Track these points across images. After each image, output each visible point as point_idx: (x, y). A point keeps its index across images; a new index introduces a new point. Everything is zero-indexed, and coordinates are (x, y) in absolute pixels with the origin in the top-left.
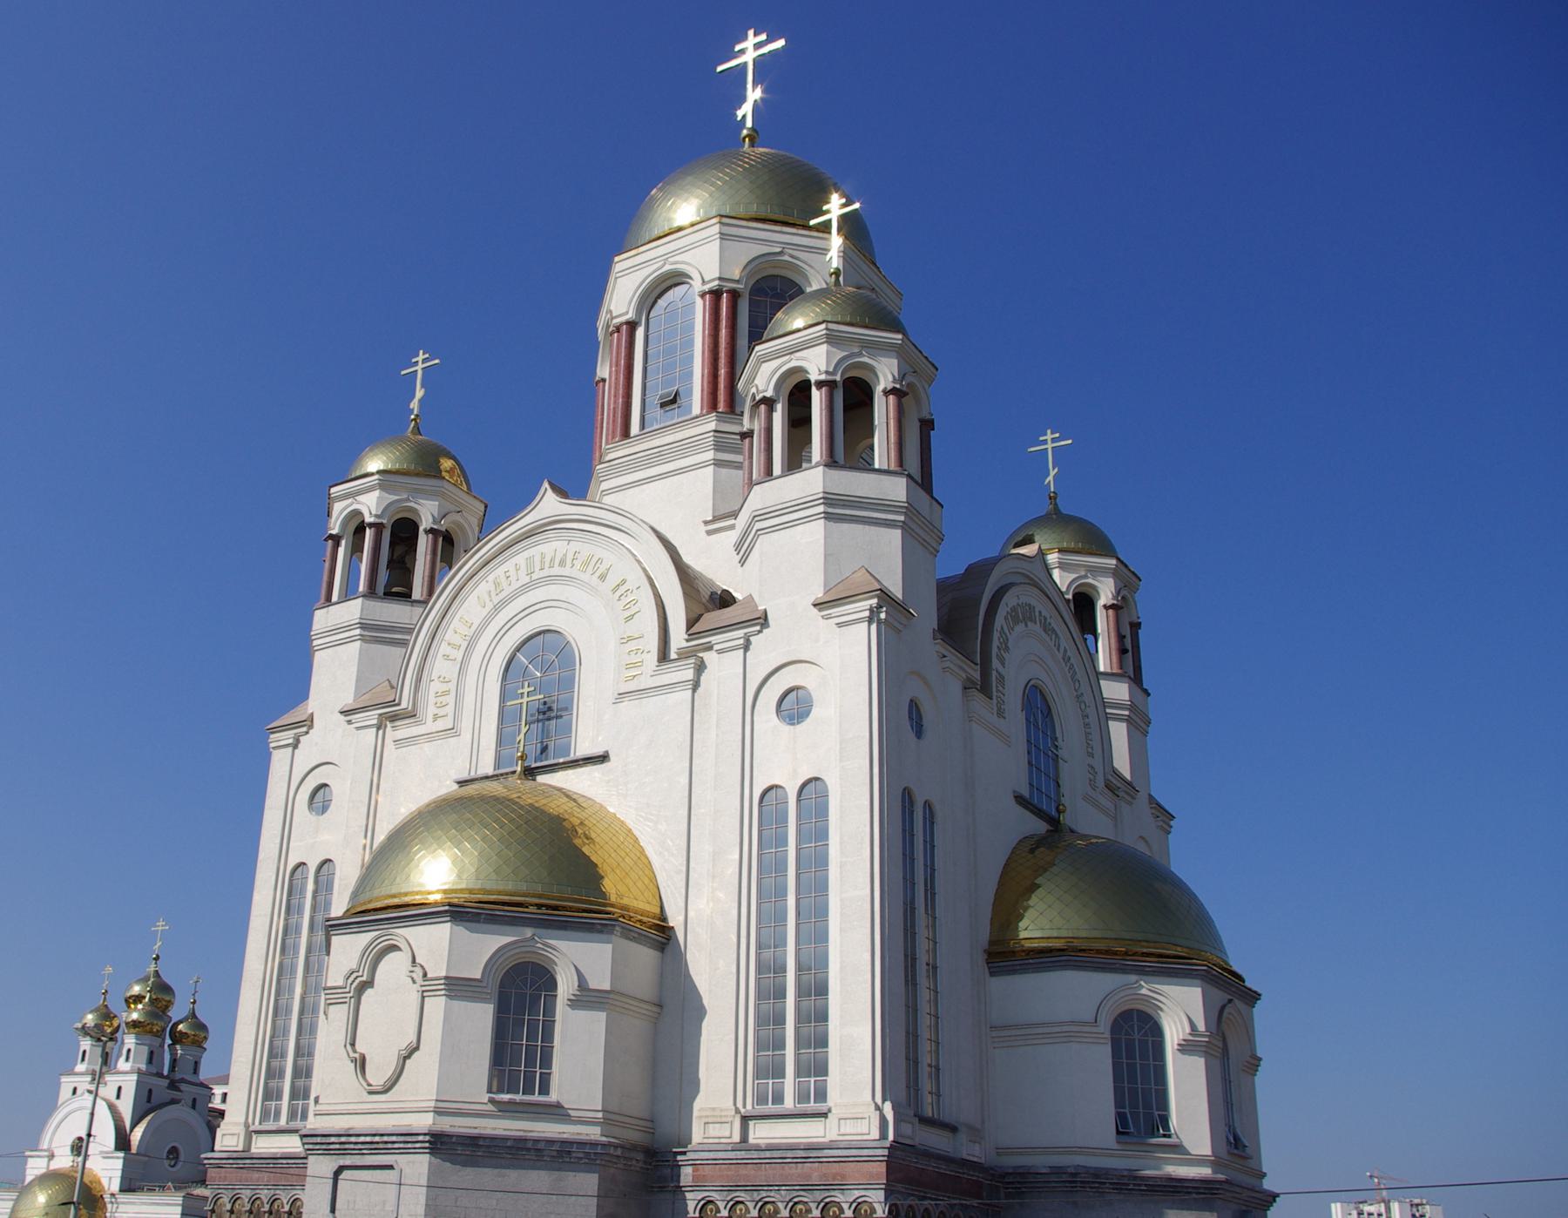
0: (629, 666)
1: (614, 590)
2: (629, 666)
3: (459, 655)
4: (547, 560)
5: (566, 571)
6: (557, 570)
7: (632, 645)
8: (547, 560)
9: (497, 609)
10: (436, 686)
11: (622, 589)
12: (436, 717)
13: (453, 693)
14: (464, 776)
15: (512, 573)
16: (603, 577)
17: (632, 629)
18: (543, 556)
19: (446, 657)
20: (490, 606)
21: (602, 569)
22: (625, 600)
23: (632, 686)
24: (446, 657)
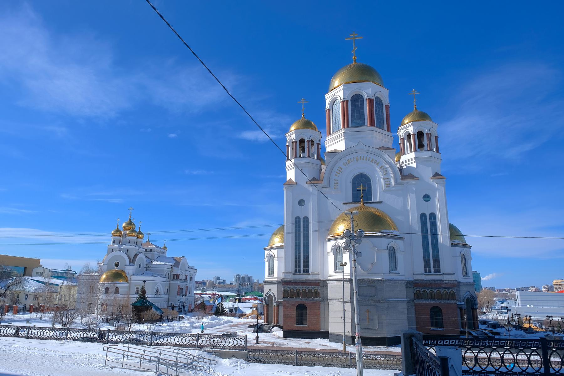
14: (344, 202)
15: (352, 159)
21: (377, 163)
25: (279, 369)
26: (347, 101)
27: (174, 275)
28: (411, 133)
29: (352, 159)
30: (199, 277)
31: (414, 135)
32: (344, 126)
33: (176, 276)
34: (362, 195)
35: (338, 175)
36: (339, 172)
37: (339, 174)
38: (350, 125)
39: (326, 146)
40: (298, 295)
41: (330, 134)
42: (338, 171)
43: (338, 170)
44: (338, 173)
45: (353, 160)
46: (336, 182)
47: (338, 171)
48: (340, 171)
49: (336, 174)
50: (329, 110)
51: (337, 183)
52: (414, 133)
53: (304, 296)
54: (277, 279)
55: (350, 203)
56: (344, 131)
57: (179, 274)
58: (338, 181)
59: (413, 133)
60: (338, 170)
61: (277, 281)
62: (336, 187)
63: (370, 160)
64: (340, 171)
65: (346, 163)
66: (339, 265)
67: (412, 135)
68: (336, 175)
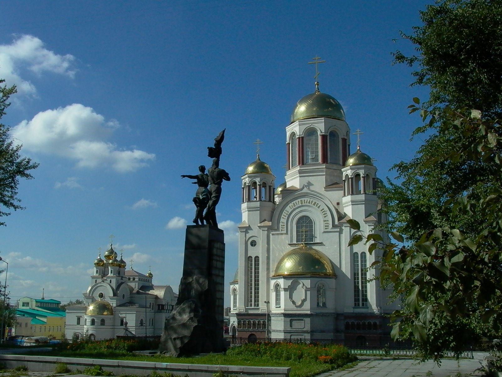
0: (326, 226)
1: (321, 210)
2: (326, 226)
3: (286, 218)
4: (306, 201)
5: (310, 205)
6: (308, 204)
7: (326, 222)
8: (306, 201)
9: (294, 210)
10: (281, 224)
11: (323, 211)
12: (282, 230)
13: (285, 226)
15: (297, 202)
16: (319, 207)
17: (326, 219)
18: (304, 200)
19: (283, 218)
20: (292, 209)
21: (318, 205)
22: (324, 213)
23: (326, 230)
24: (283, 218)
27: (159, 305)
29: (297, 202)
32: (299, 164)
33: (161, 306)
35: (285, 217)
37: (286, 216)
39: (287, 181)
41: (289, 169)
44: (285, 216)
45: (298, 204)
48: (287, 214)
50: (289, 144)
56: (299, 169)
57: (163, 304)
61: (236, 314)
62: (283, 229)
63: (313, 203)
65: (292, 206)
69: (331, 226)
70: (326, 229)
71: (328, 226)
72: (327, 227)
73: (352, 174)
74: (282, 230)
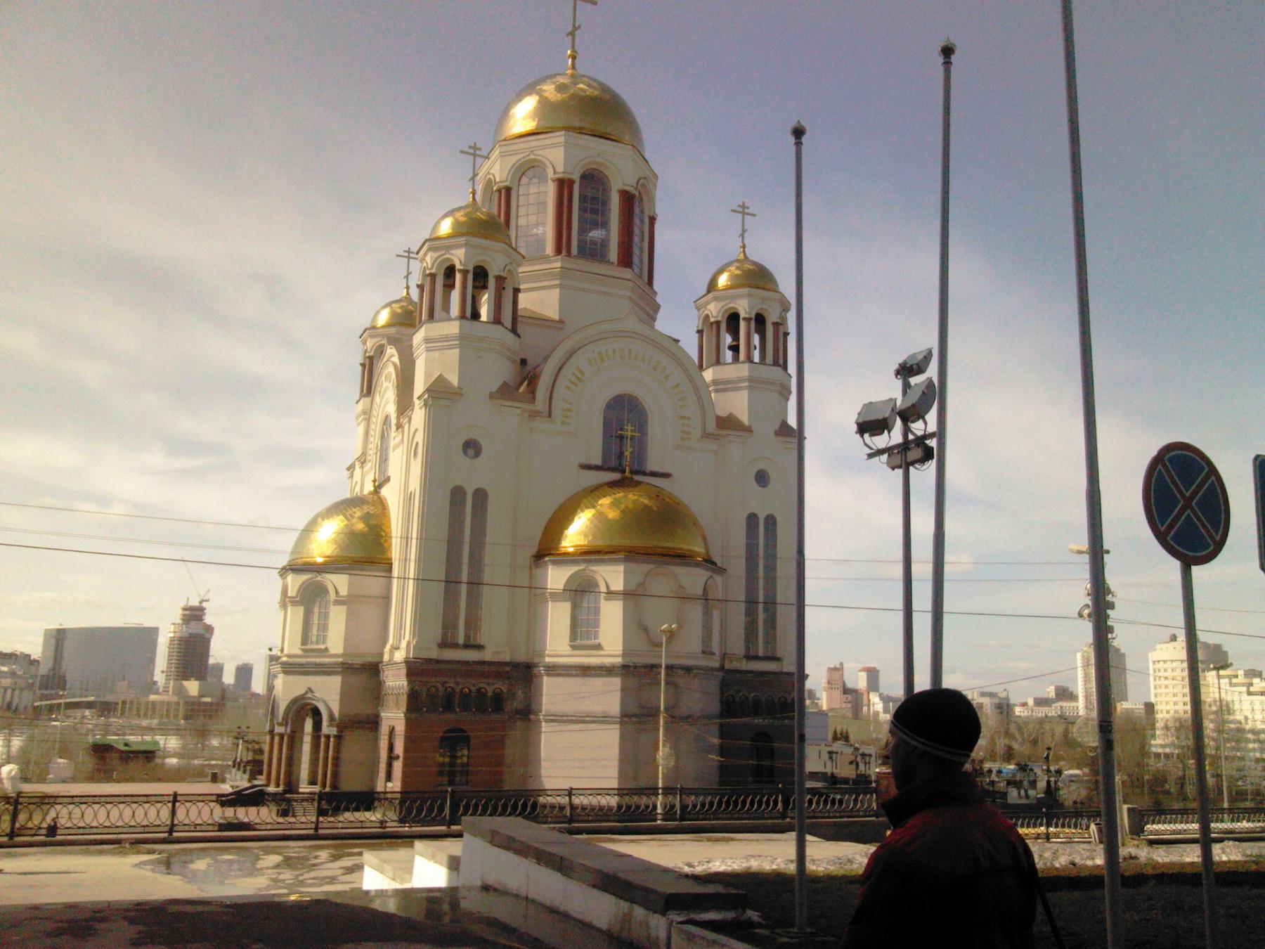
1: (673, 388)
2: (683, 432)
7: (685, 421)
14: (583, 461)
16: (667, 377)
18: (630, 351)
25: (848, 867)
26: (571, 182)
28: (458, 266)
30: (737, 645)
31: (748, 320)
32: (558, 251)
34: (630, 450)
36: (576, 381)
38: (574, 250)
40: (448, 705)
42: (574, 379)
43: (573, 374)
46: (567, 406)
47: (574, 379)
48: (579, 379)
49: (570, 385)
51: (569, 410)
52: (466, 268)
53: (465, 707)
54: (341, 660)
55: (597, 468)
58: (571, 404)
59: (462, 268)
60: (573, 374)
61: (342, 663)
64: (579, 379)
65: (595, 359)
66: (581, 629)
67: (460, 271)
68: (568, 388)
69: (696, 433)
70: (683, 439)
71: (688, 433)
72: (685, 436)
73: (719, 312)
74: (563, 423)
